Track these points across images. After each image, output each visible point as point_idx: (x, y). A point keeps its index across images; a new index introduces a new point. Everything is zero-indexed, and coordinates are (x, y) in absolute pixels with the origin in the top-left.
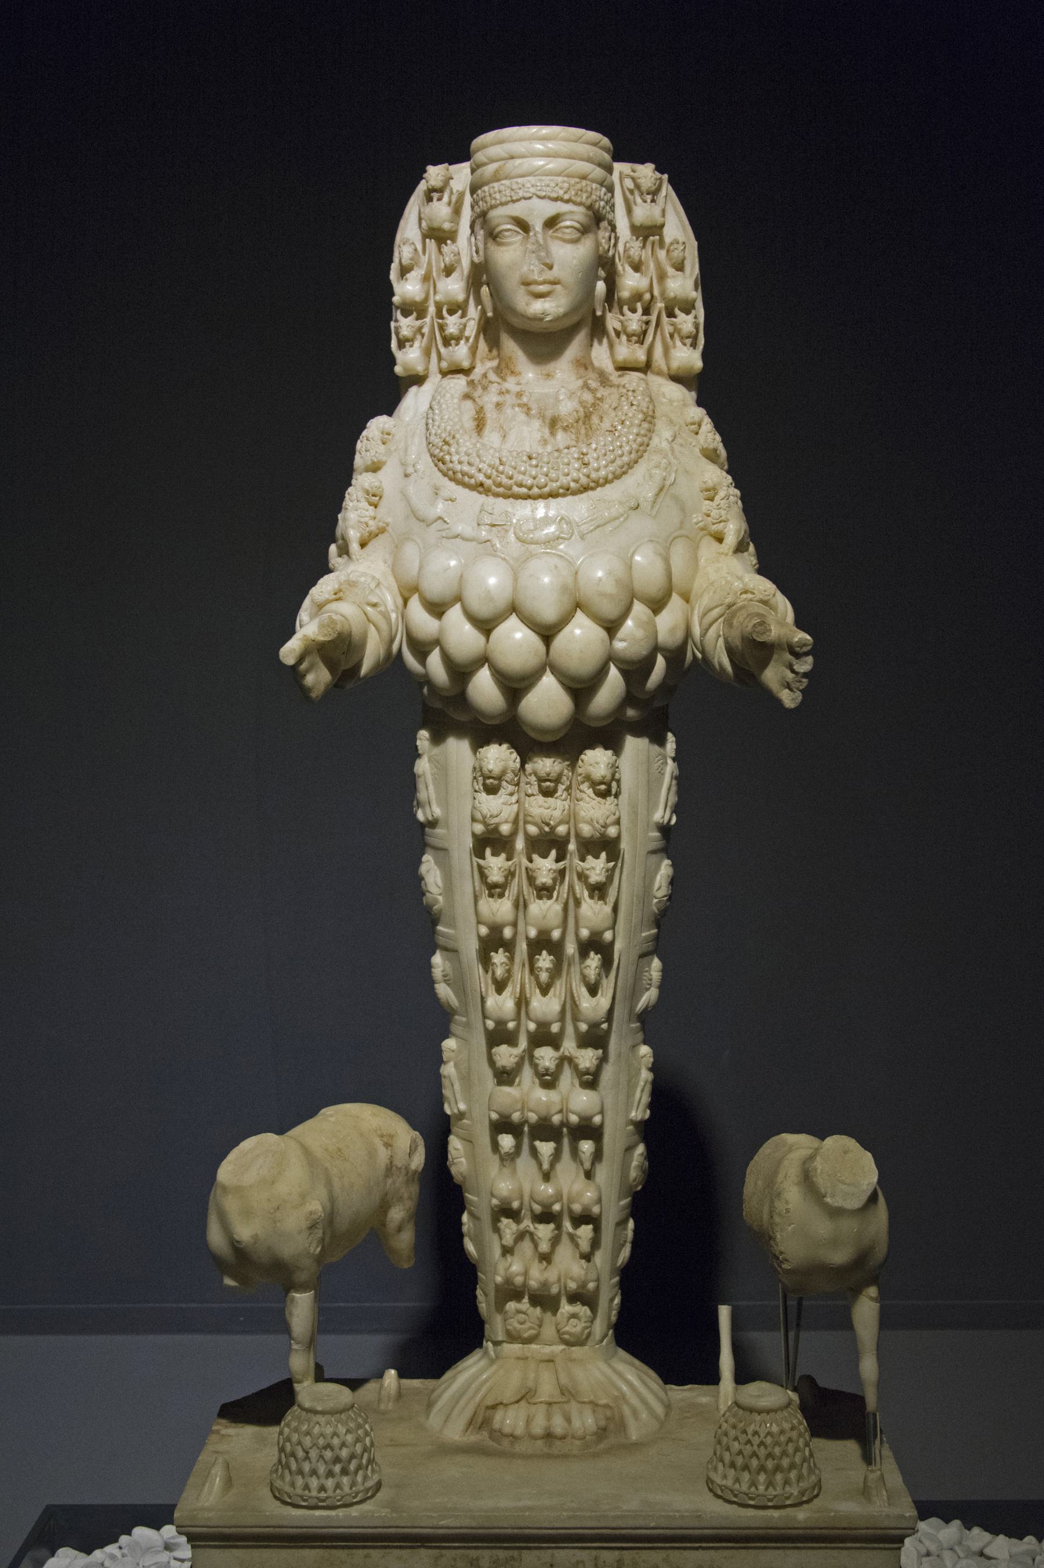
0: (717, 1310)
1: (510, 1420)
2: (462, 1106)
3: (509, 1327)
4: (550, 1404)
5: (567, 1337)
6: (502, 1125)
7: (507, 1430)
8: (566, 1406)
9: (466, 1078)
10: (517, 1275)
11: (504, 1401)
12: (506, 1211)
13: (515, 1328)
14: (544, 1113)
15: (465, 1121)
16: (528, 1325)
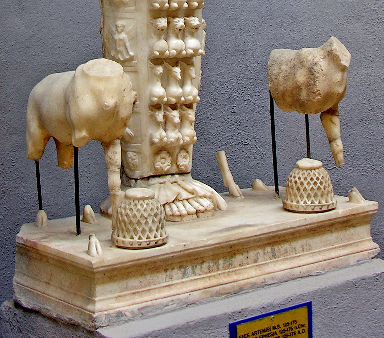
0: (218, 155)
1: (179, 208)
2: (132, 53)
3: (158, 166)
4: (187, 200)
5: (183, 167)
6: (157, 61)
7: (178, 213)
8: (195, 199)
9: (134, 39)
10: (165, 137)
11: (169, 202)
12: (156, 107)
13: (161, 167)
14: (179, 49)
15: (133, 62)
16: (167, 164)
